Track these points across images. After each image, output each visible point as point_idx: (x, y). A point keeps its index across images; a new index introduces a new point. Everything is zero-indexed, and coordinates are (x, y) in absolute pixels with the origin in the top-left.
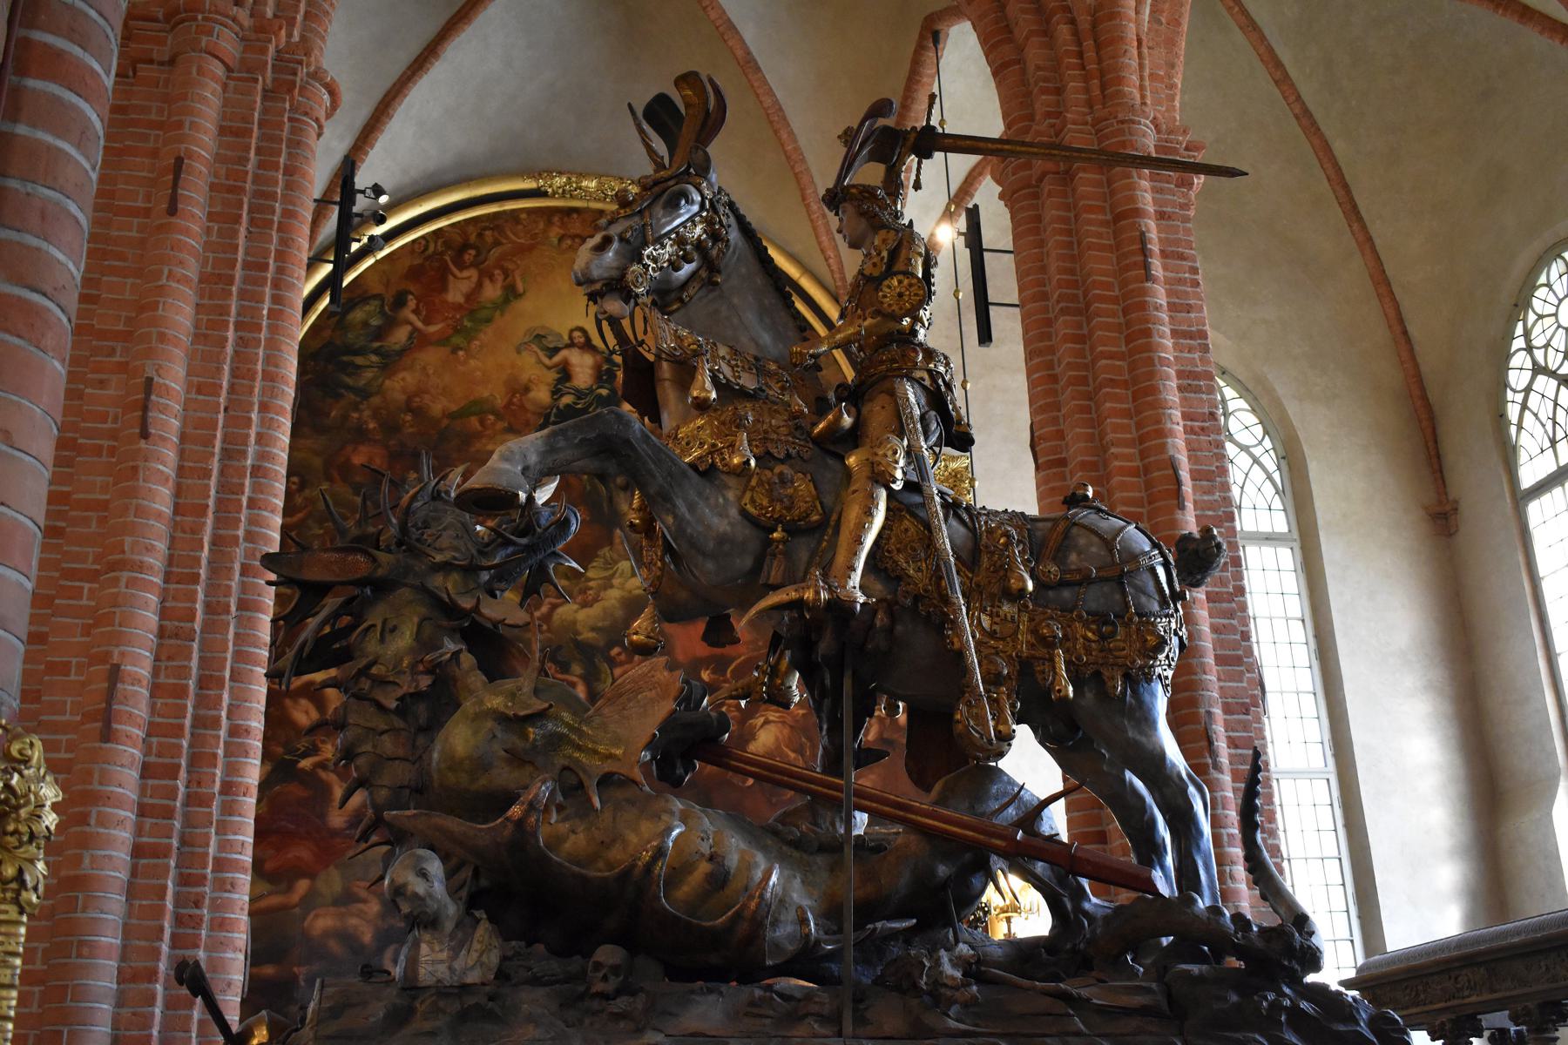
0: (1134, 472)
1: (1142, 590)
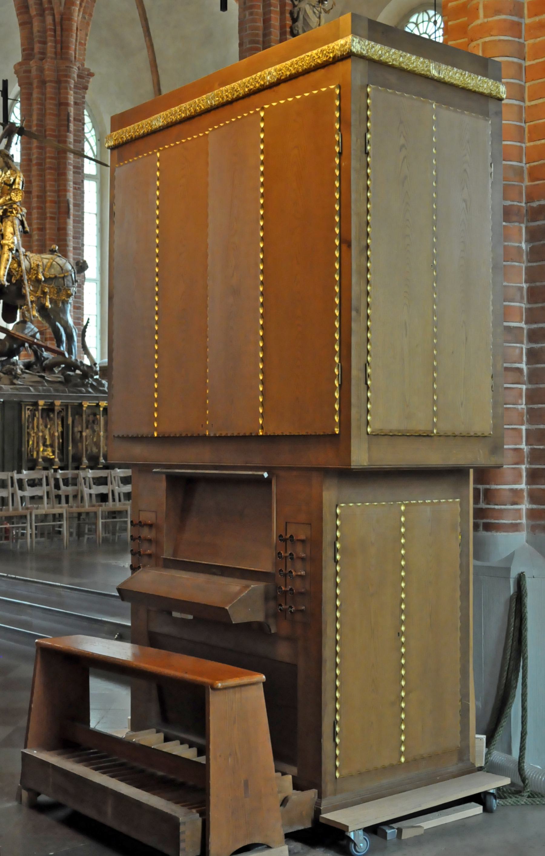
0: (54, 202)
1: (68, 280)
